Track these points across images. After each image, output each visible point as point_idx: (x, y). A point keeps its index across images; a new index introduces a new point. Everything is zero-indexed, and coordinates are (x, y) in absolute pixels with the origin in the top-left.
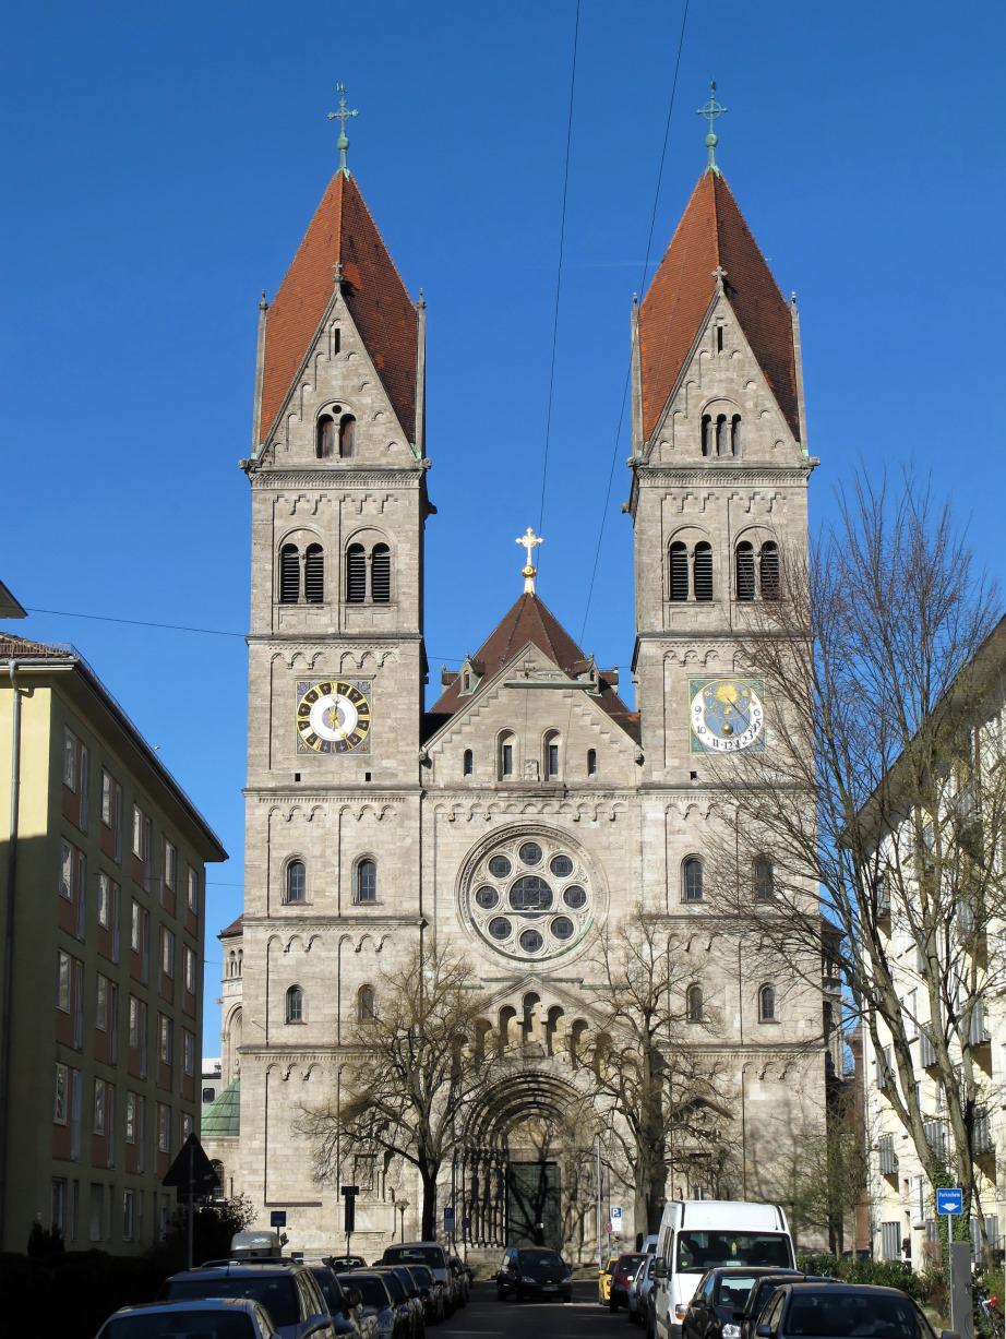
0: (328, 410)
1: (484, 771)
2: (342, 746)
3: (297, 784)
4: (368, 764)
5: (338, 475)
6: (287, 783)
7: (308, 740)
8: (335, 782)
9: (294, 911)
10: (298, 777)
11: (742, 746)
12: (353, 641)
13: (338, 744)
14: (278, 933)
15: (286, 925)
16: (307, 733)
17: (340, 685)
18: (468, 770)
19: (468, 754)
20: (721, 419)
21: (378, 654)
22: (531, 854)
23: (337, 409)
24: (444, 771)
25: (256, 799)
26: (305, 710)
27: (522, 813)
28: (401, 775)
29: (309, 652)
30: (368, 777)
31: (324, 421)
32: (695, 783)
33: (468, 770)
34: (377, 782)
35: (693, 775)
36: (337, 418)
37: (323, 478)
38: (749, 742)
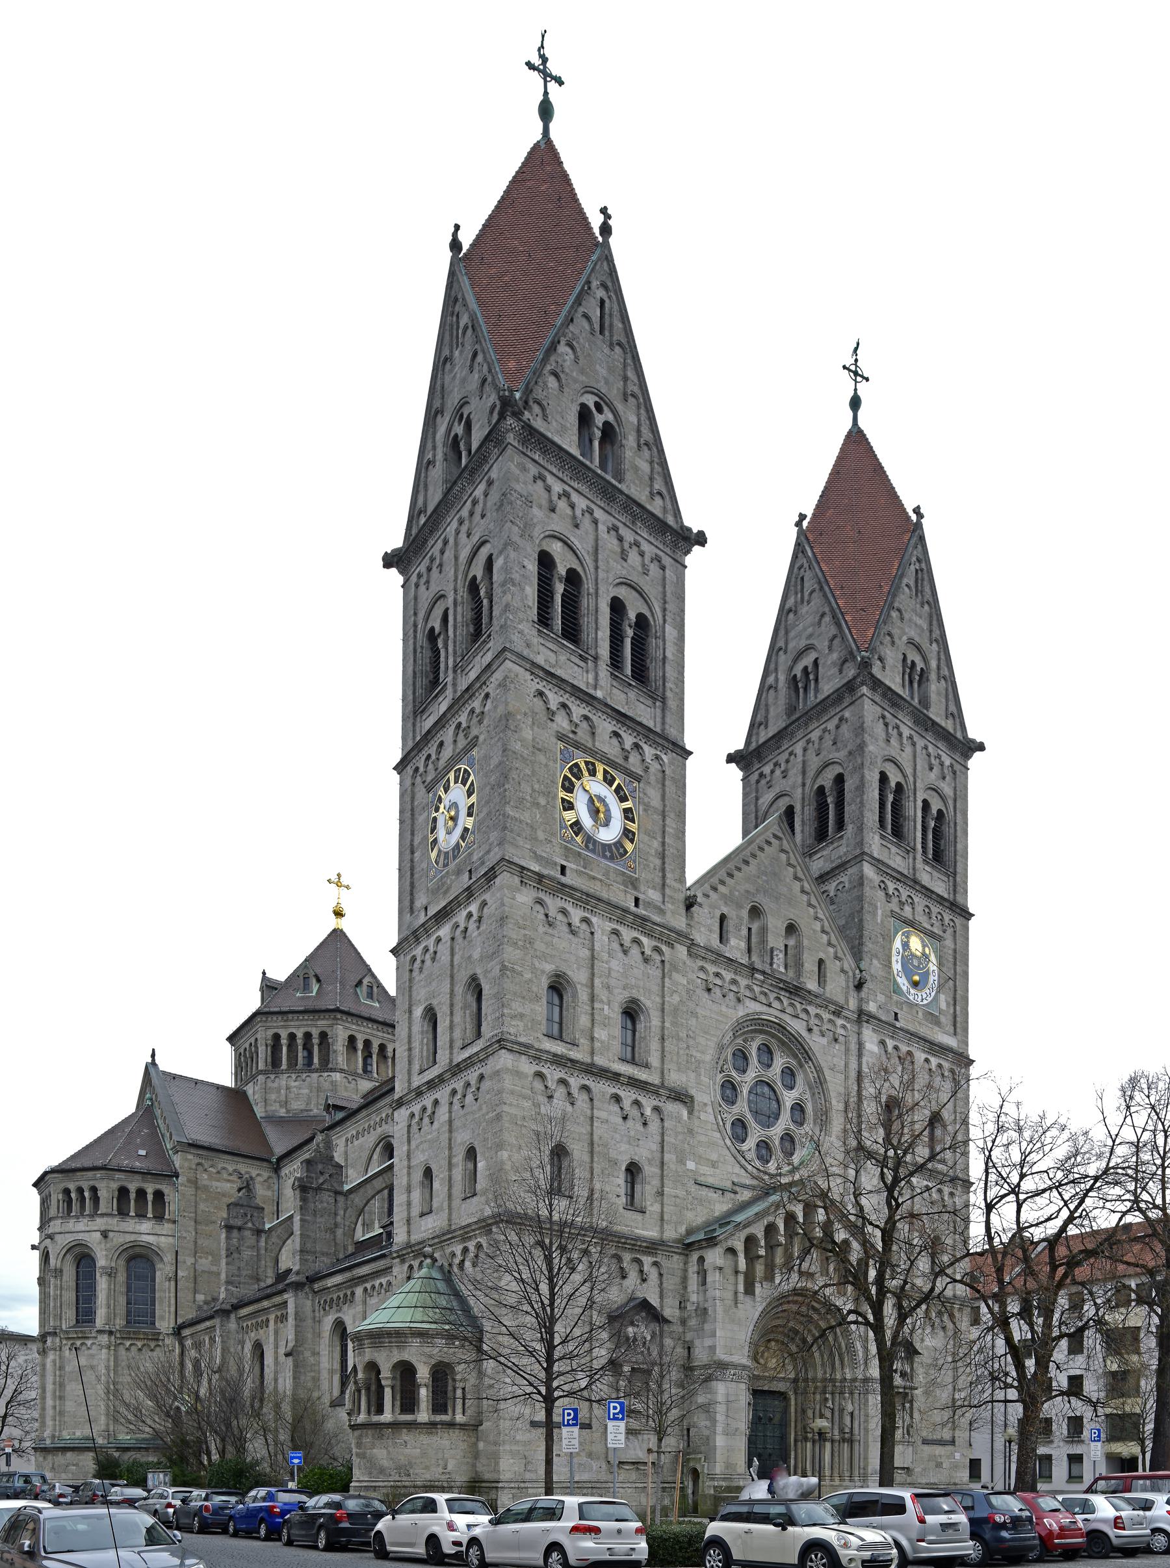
6: (552, 873)
7: (571, 826)
9: (558, 1048)
12: (622, 719)
14: (544, 1071)
15: (552, 1063)
16: (569, 816)
19: (723, 918)
21: (649, 751)
24: (702, 929)
25: (517, 880)
26: (569, 788)
27: (770, 1006)
28: (669, 914)
29: (578, 710)
34: (644, 912)
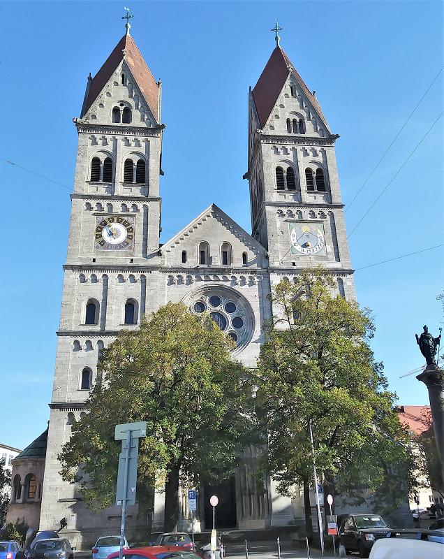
0: (118, 105)
1: (193, 261)
2: (119, 246)
3: (94, 264)
4: (132, 255)
5: (121, 129)
8: (115, 263)
10: (94, 260)
11: (315, 252)
13: (117, 245)
17: (118, 219)
18: (184, 261)
19: (184, 254)
20: (294, 121)
22: (215, 301)
23: (122, 105)
30: (132, 260)
31: (116, 110)
32: (295, 267)
33: (184, 261)
35: (294, 264)
36: (122, 108)
37: (114, 130)
38: (318, 250)
